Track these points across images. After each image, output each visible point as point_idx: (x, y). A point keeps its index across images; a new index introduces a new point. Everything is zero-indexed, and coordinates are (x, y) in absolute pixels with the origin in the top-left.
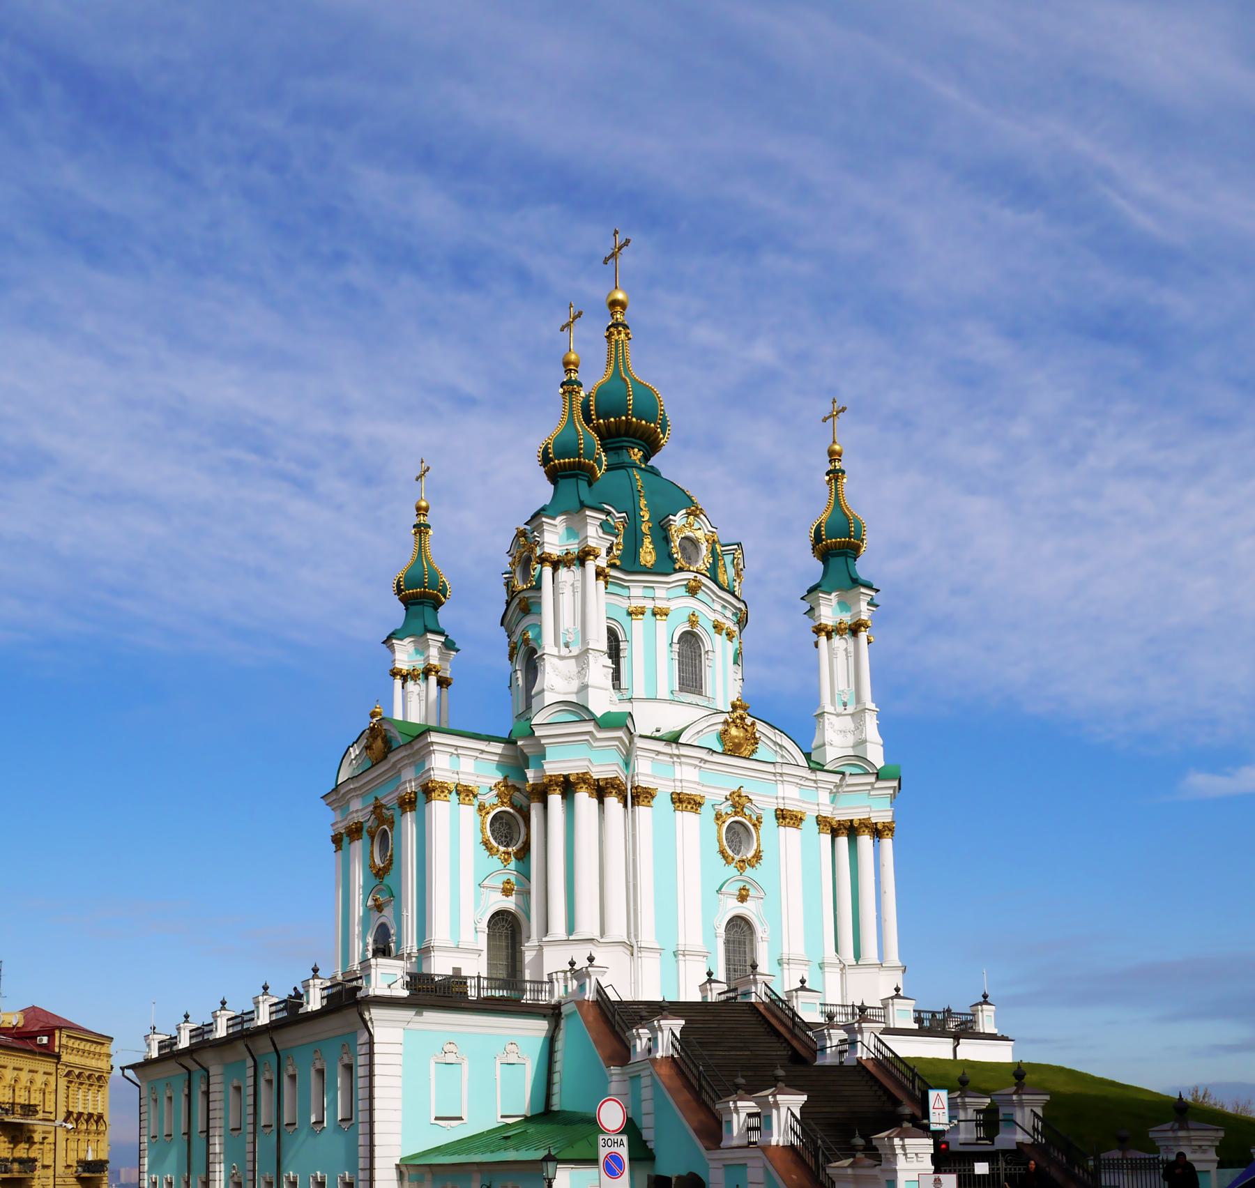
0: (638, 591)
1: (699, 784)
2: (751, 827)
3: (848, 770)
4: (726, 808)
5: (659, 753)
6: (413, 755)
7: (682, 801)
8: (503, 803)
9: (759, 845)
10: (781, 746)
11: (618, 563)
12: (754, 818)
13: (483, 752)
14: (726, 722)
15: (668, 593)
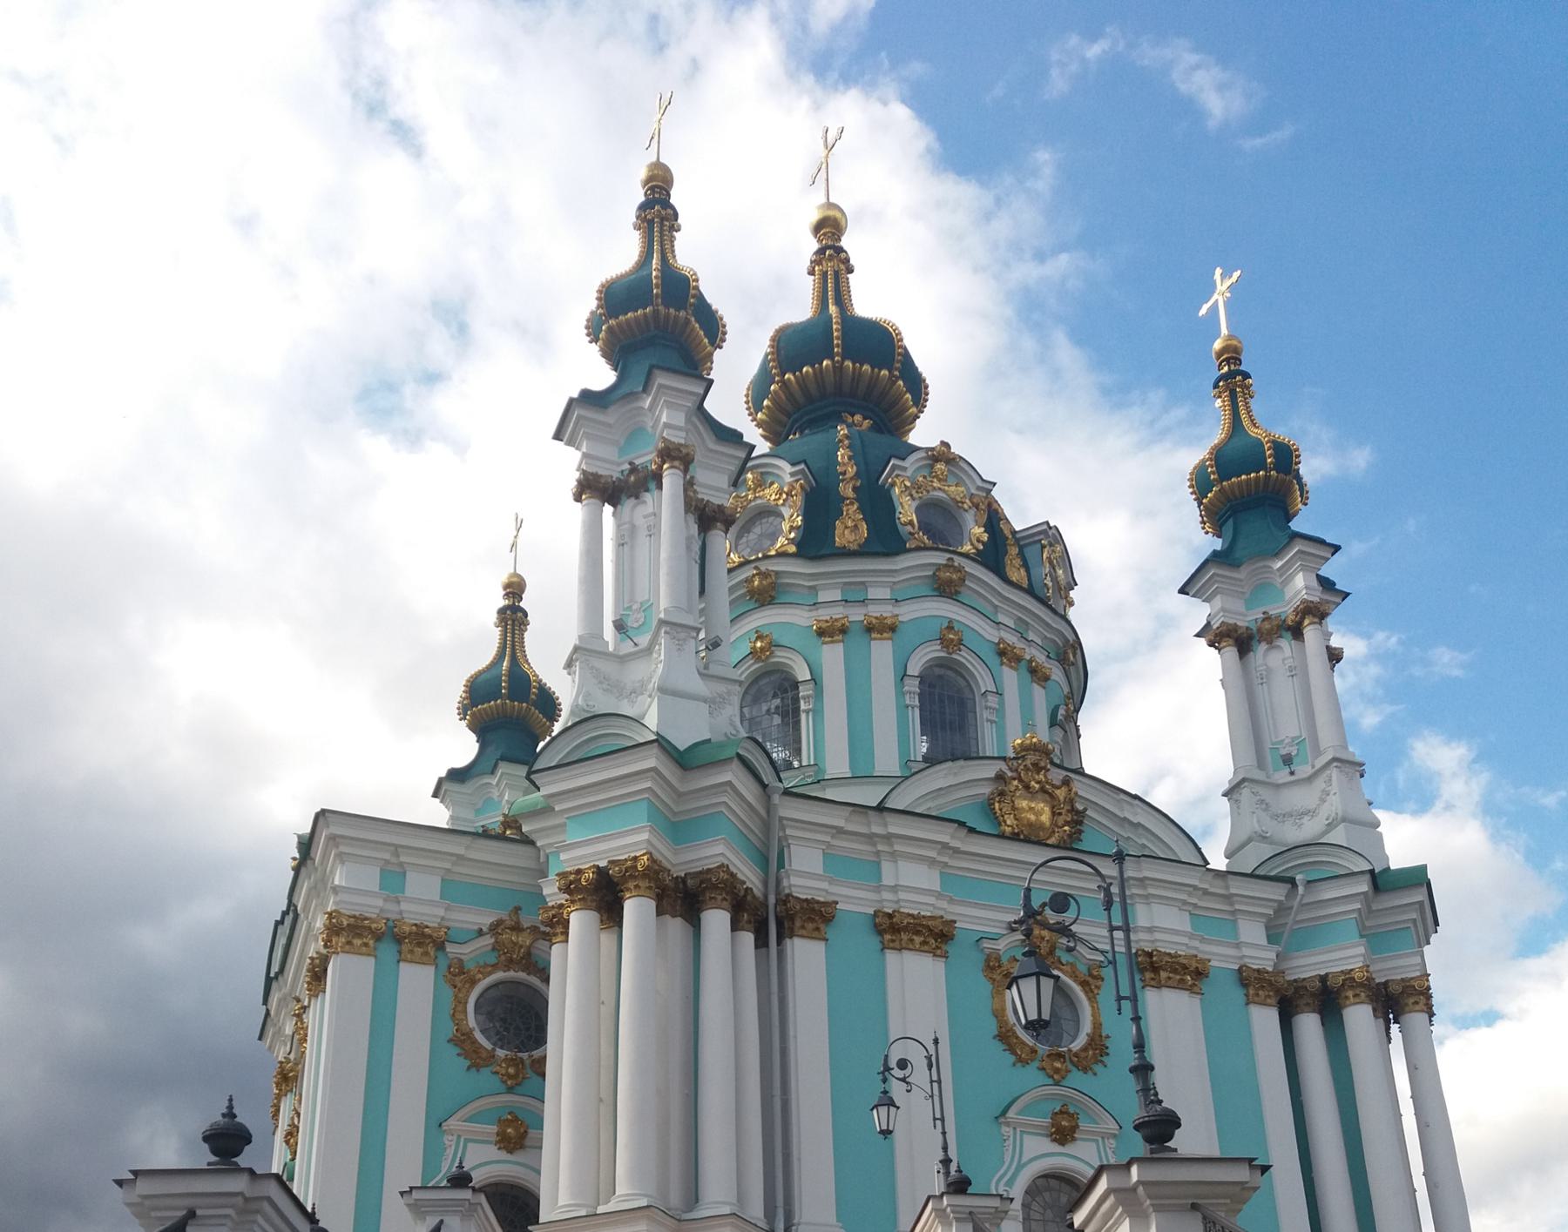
0: (829, 589)
1: (939, 896)
2: (1077, 989)
3: (1298, 877)
4: (1009, 945)
5: (840, 831)
6: (324, 879)
7: (895, 930)
8: (509, 964)
9: (1097, 1025)
10: (1139, 825)
11: (792, 549)
12: (1082, 969)
13: (460, 857)
14: (1000, 777)
15: (891, 586)
